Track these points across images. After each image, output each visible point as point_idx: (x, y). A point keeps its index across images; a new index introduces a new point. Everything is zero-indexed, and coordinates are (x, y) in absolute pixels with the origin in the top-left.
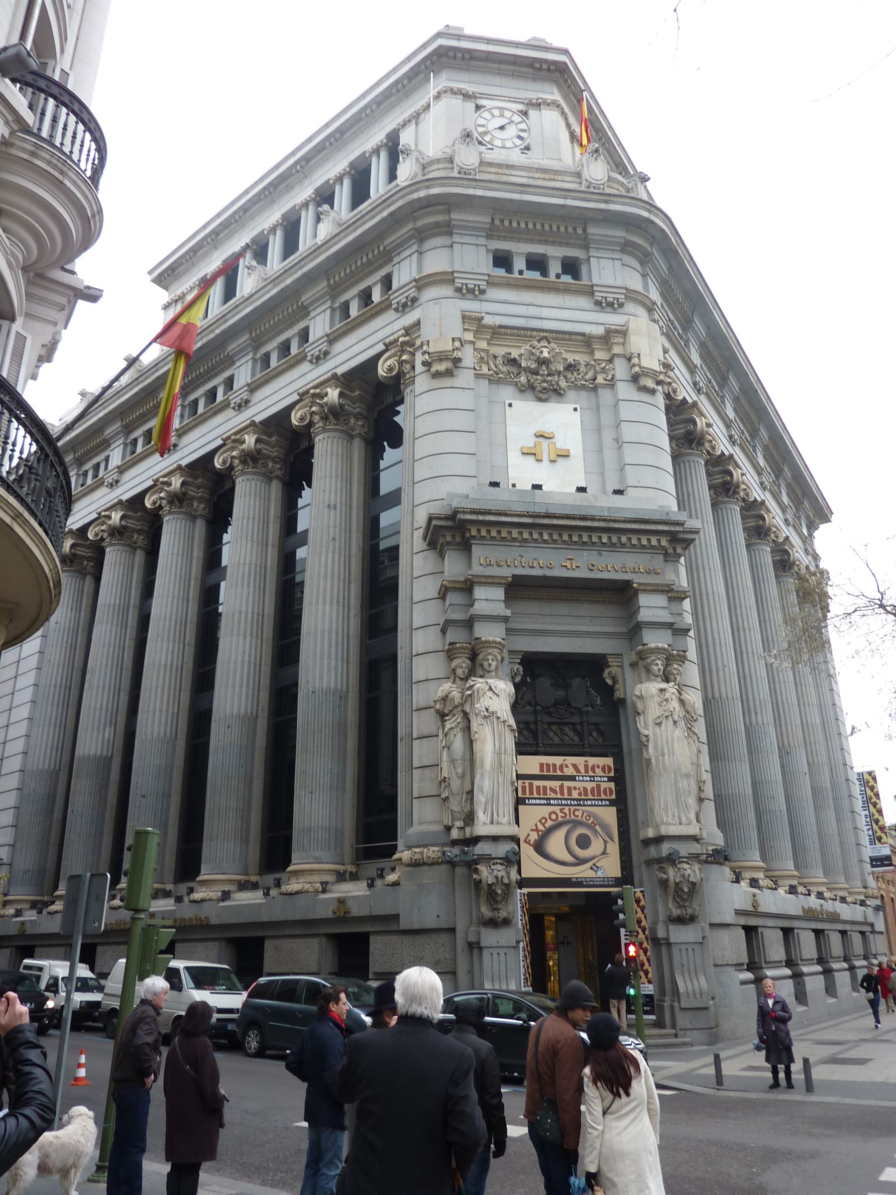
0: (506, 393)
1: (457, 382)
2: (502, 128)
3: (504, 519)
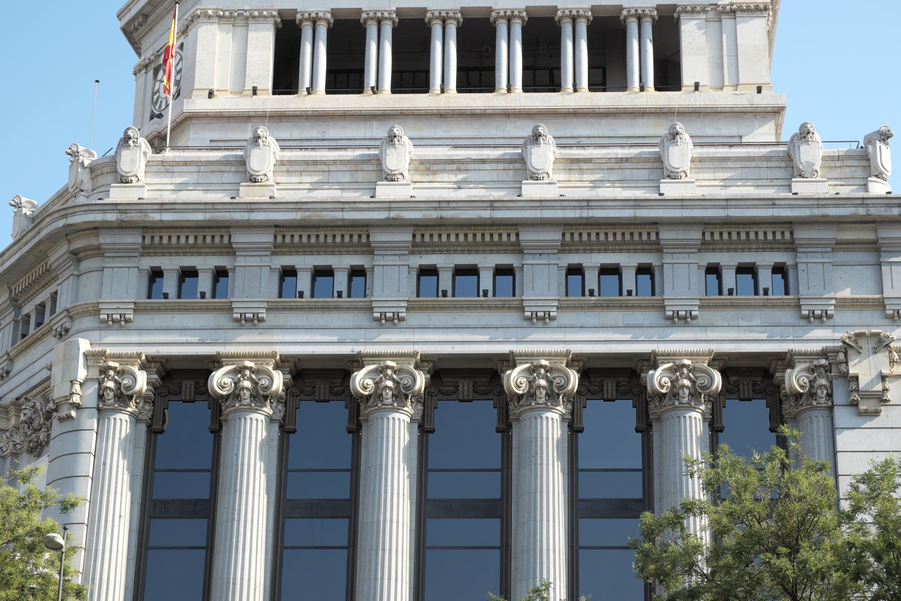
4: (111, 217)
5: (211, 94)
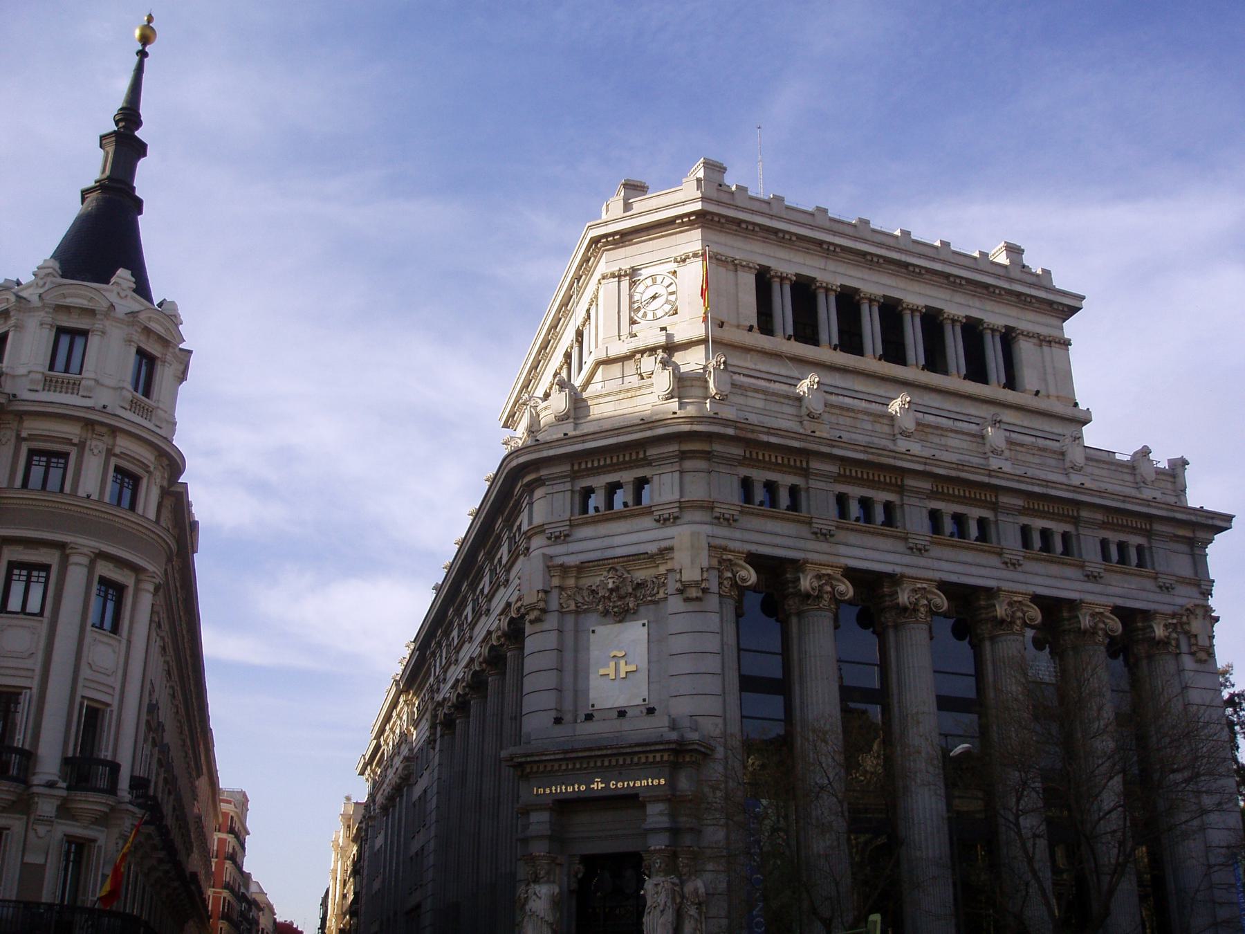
0: (591, 620)
1: (546, 626)
2: (654, 297)
3: (544, 758)
4: (731, 431)
5: (722, 325)
